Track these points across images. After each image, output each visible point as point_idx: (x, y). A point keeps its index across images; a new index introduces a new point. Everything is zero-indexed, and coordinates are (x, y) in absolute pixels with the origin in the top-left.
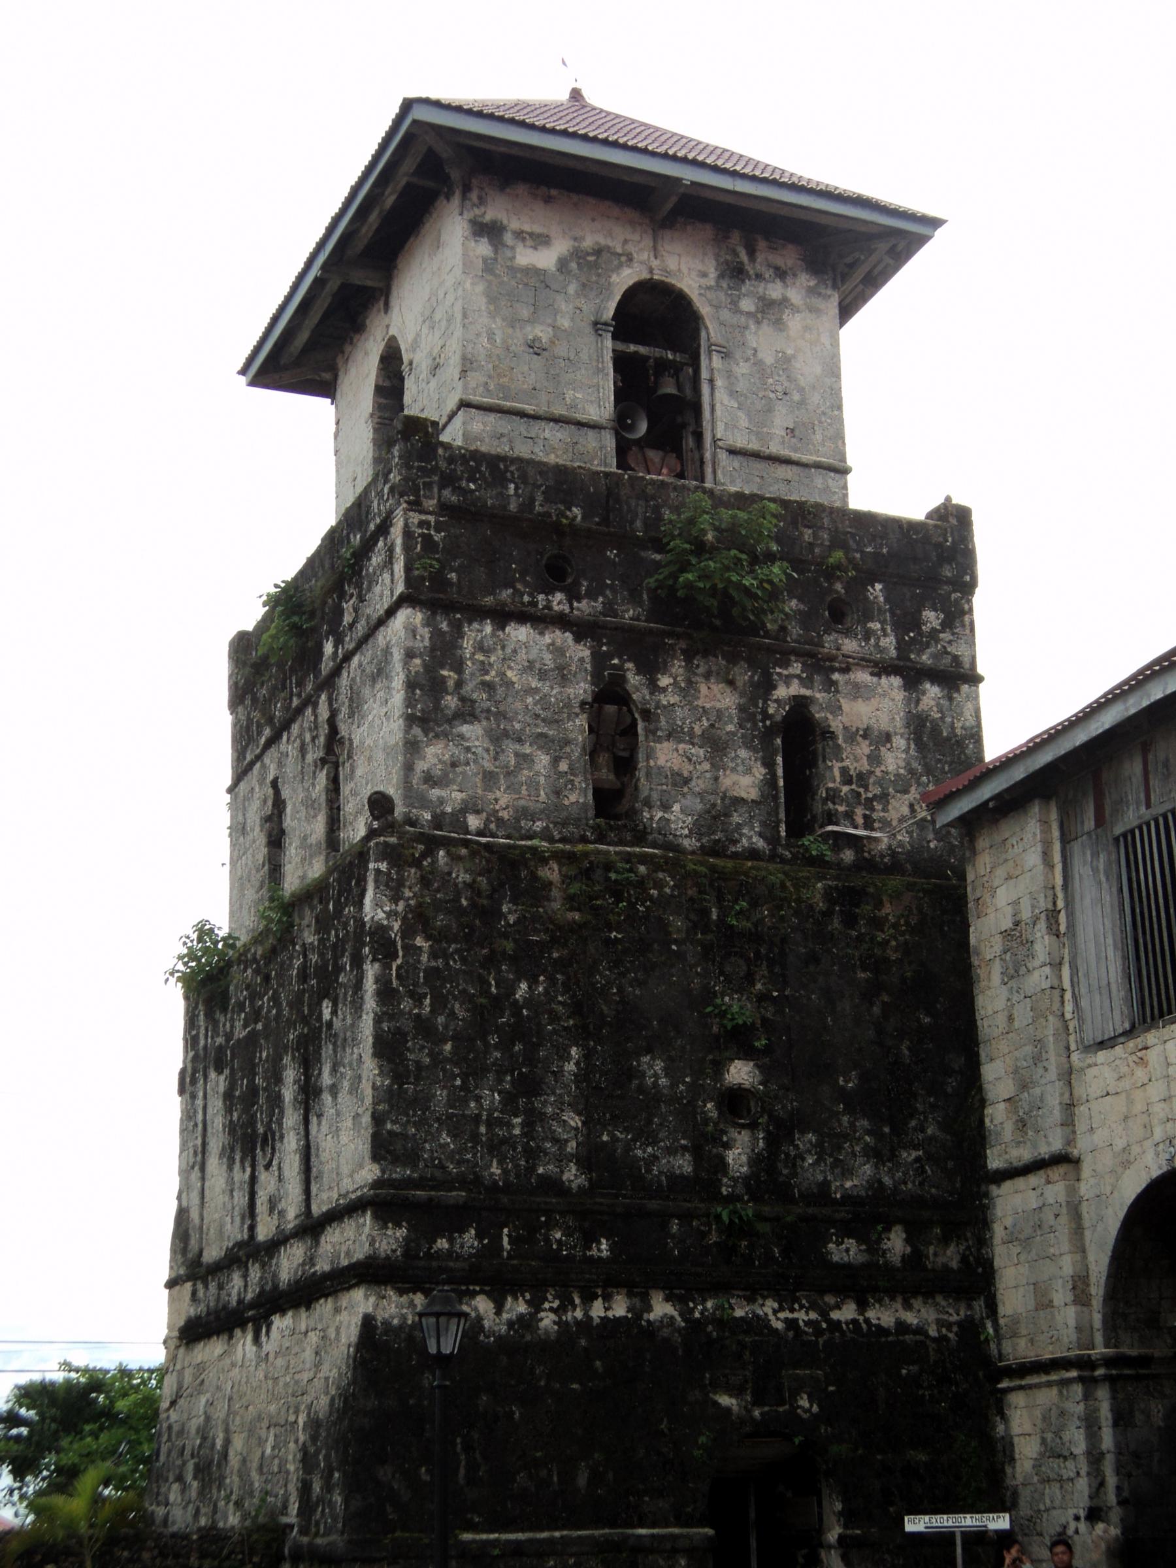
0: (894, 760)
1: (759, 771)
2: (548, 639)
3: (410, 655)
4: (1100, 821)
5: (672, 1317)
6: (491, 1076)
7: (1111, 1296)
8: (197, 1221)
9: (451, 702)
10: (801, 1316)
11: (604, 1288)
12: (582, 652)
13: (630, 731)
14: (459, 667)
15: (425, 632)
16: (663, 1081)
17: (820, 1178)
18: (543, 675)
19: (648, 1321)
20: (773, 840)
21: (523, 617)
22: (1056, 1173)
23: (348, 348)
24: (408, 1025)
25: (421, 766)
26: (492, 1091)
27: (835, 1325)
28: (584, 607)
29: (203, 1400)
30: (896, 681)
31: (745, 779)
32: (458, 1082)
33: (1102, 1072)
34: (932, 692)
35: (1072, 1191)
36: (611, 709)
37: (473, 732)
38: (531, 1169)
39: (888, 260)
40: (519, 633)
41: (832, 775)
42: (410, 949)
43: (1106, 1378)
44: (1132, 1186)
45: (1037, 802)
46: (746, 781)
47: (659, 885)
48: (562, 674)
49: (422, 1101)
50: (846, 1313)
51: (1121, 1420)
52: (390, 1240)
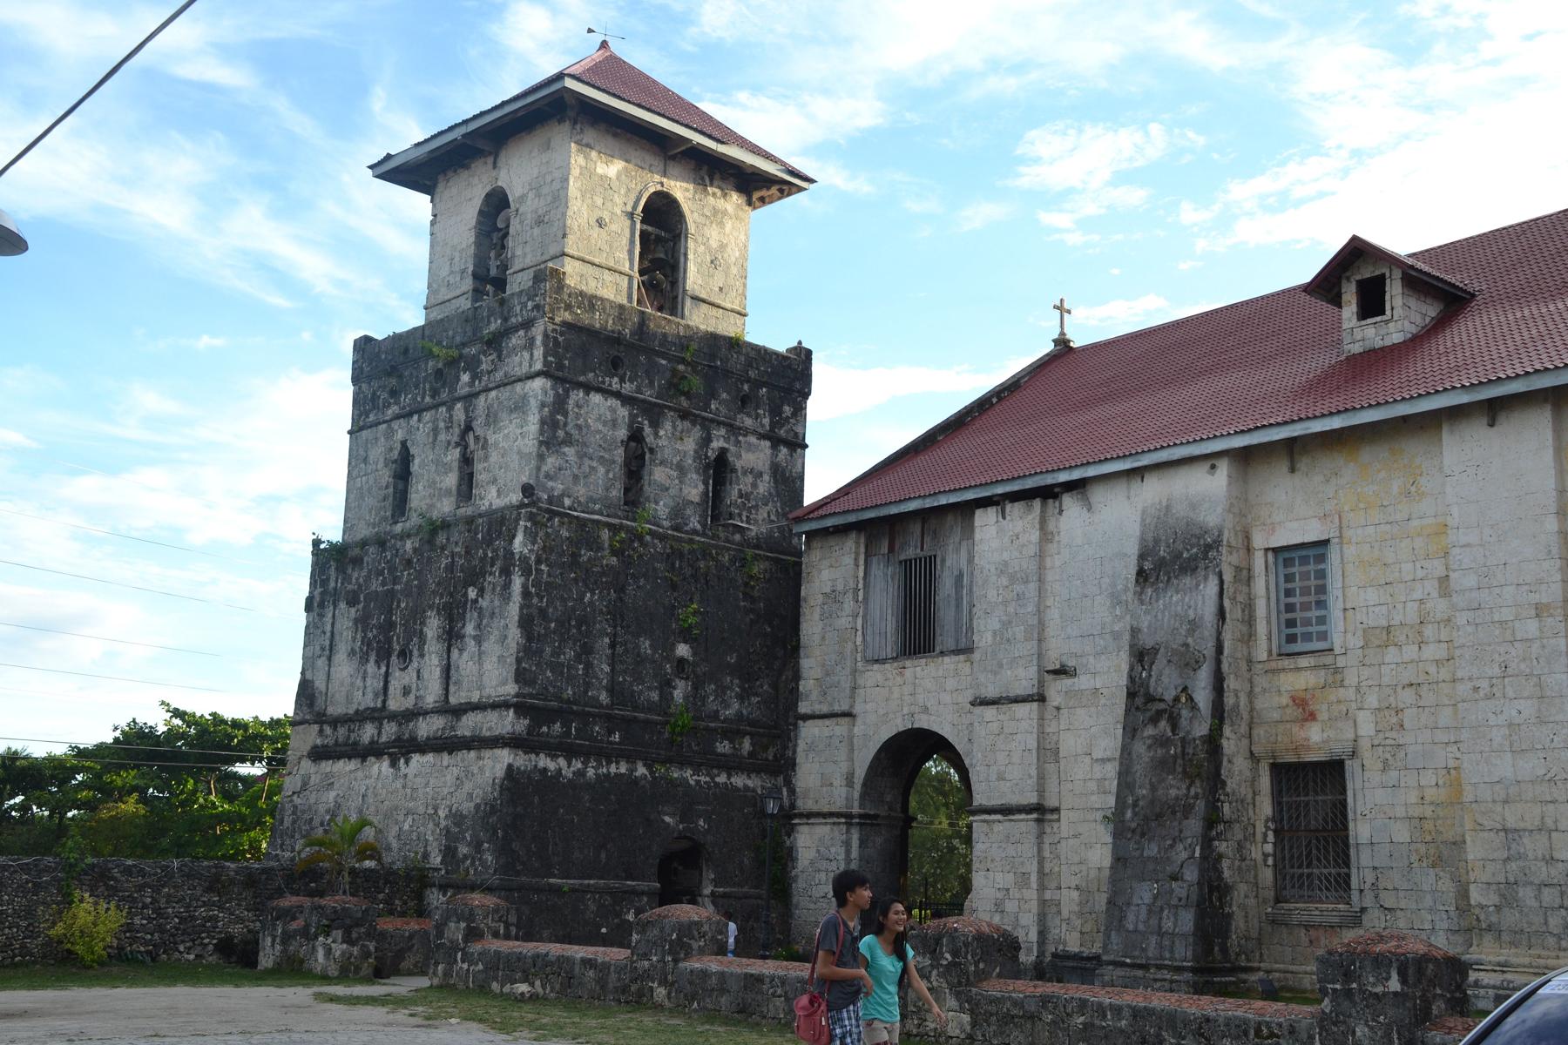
0: (764, 486)
1: (701, 487)
2: (609, 402)
3: (543, 405)
4: (891, 549)
7: (864, 785)
8: (323, 688)
9: (561, 433)
10: (702, 779)
12: (624, 413)
13: (642, 456)
14: (566, 414)
15: (551, 393)
18: (605, 423)
20: (704, 526)
21: (599, 390)
23: (450, 174)
24: (535, 612)
25: (545, 468)
27: (717, 784)
28: (628, 388)
29: (332, 794)
30: (768, 443)
31: (694, 490)
33: (875, 674)
34: (784, 450)
35: (850, 731)
36: (633, 444)
37: (570, 451)
38: (586, 692)
40: (596, 398)
41: (733, 494)
42: (539, 571)
43: (860, 824)
44: (886, 734)
46: (694, 492)
47: (655, 547)
48: (614, 424)
49: (540, 652)
50: (722, 779)
51: (863, 843)
52: (522, 725)
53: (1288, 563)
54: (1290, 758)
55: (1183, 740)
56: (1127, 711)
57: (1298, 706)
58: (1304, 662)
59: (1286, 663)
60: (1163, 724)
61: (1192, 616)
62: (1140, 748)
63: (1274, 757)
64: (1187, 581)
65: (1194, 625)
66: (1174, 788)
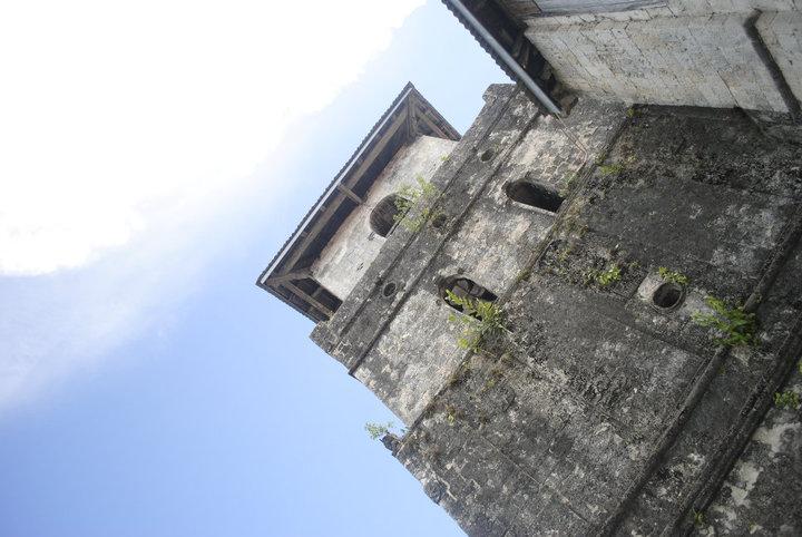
1: (520, 218)
5: (787, 431)
6: (541, 470)
9: (394, 374)
11: (726, 477)
16: (618, 347)
17: (751, 254)
19: (777, 455)
22: (760, 26)
25: (403, 409)
26: (549, 475)
32: (526, 497)
37: (412, 369)
38: (612, 480)
39: (428, 112)
40: (394, 326)
45: (526, 34)
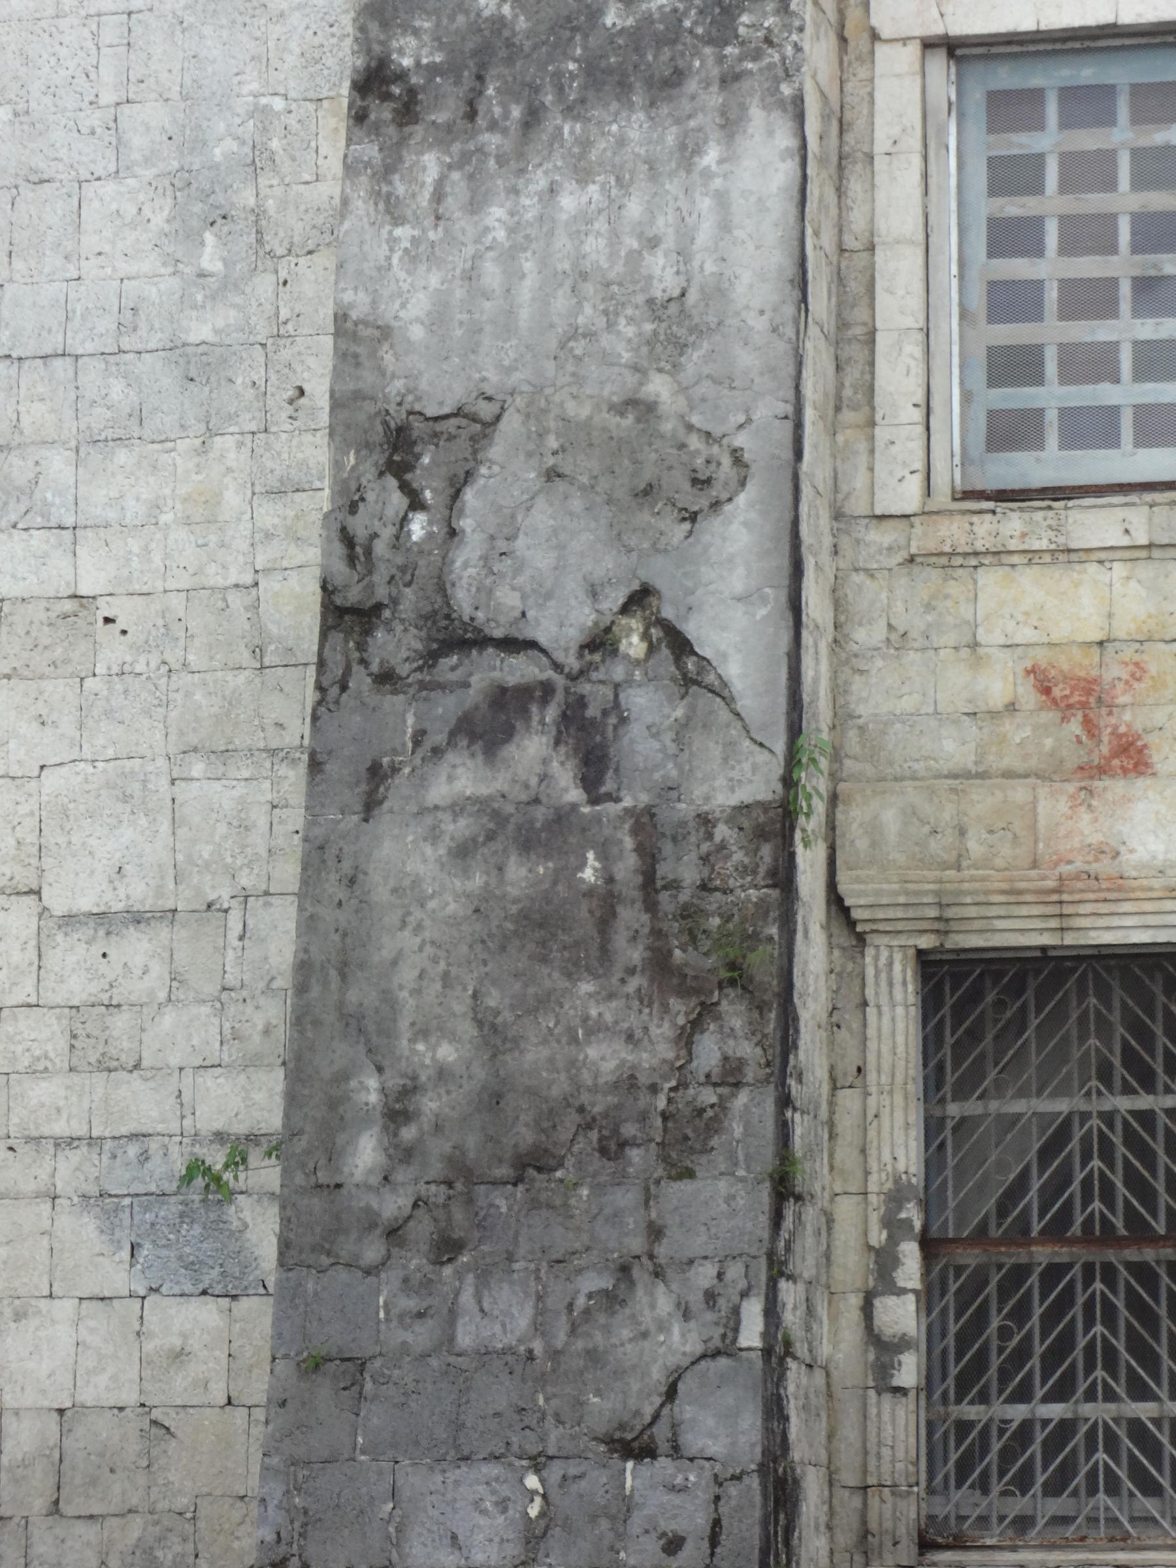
53: (1011, 110)
54: (1022, 930)
55: (644, 823)
56: (330, 691)
57: (1065, 709)
58: (1097, 525)
59: (1013, 525)
60: (534, 750)
61: (663, 273)
62: (409, 855)
63: (943, 925)
64: (633, 129)
65: (676, 325)
66: (610, 1038)
